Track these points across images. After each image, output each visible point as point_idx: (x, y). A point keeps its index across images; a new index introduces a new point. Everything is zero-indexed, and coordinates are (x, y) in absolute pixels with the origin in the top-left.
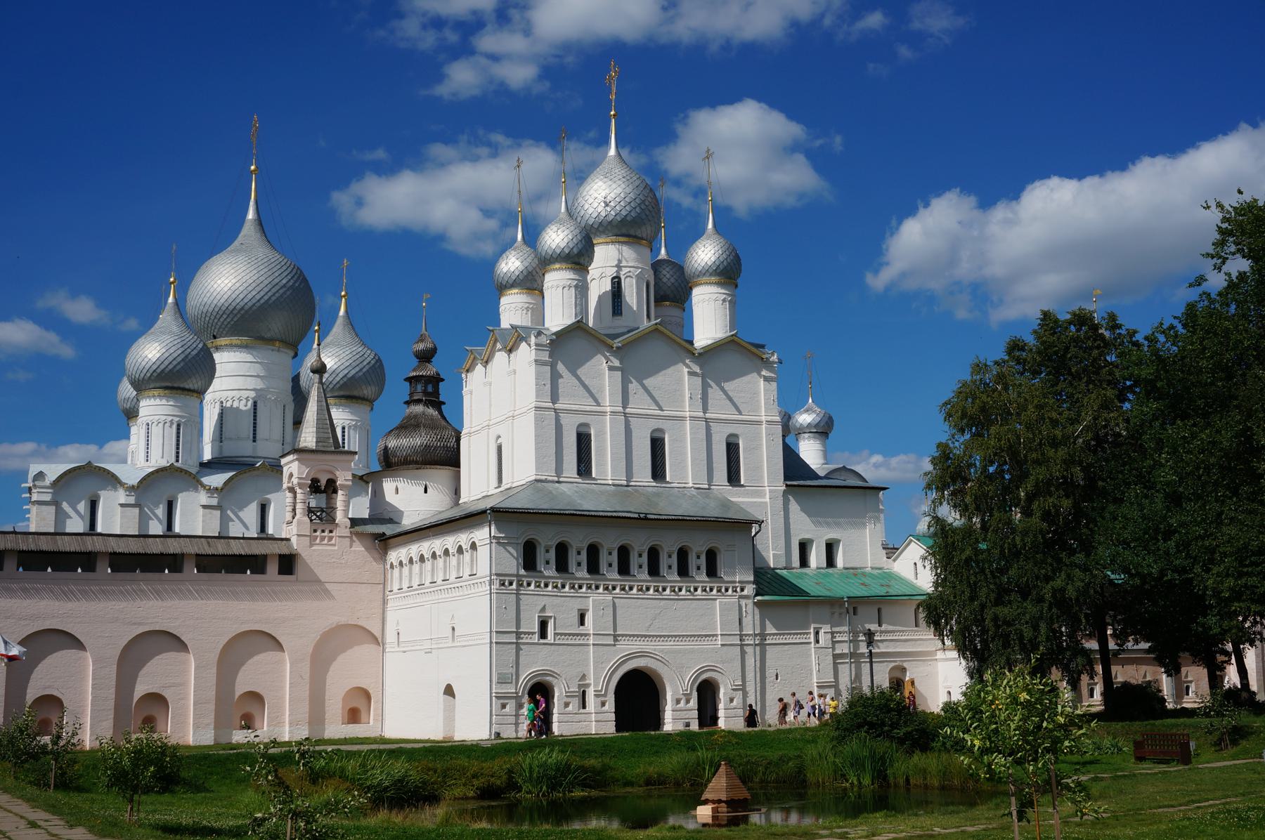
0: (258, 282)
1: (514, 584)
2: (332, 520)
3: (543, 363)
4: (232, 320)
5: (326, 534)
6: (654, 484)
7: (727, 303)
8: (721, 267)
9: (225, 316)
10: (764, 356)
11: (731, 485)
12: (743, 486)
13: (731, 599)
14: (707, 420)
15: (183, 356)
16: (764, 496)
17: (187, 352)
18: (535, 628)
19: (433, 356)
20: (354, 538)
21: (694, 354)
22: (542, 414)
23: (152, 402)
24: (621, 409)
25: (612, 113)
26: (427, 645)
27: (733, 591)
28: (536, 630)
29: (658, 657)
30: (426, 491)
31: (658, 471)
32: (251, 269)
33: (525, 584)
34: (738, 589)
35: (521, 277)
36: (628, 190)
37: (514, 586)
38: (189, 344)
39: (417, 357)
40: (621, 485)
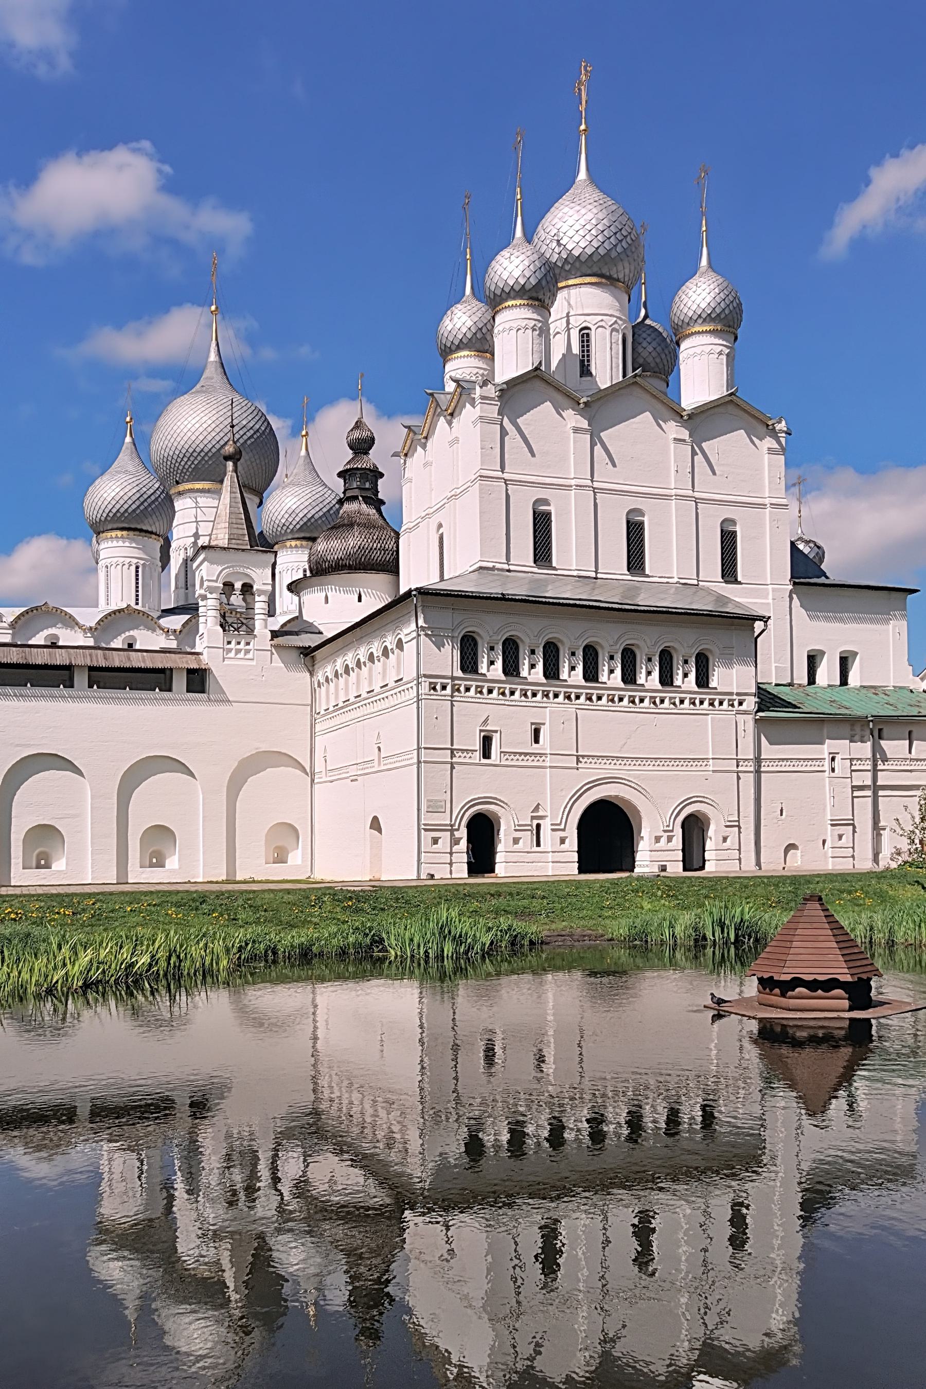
0: (218, 422)
1: (449, 688)
2: (250, 631)
3: (491, 422)
4: (193, 463)
5: (242, 646)
6: (630, 578)
7: (724, 357)
8: (718, 310)
9: (185, 459)
10: (770, 423)
11: (726, 582)
12: (740, 583)
13: (724, 716)
14: (697, 501)
15: (138, 495)
16: (767, 598)
17: (142, 492)
18: (475, 745)
19: (370, 448)
20: (274, 651)
21: (682, 416)
22: (489, 485)
23: (110, 544)
24: (589, 483)
25: (583, 127)
26: (353, 771)
27: (729, 705)
28: (477, 748)
29: (633, 785)
30: (360, 600)
31: (635, 561)
32: (210, 409)
33: (462, 689)
34: (736, 703)
35: (469, 336)
36: (601, 216)
37: (449, 690)
38: (146, 482)
39: (351, 448)
40: (589, 577)
